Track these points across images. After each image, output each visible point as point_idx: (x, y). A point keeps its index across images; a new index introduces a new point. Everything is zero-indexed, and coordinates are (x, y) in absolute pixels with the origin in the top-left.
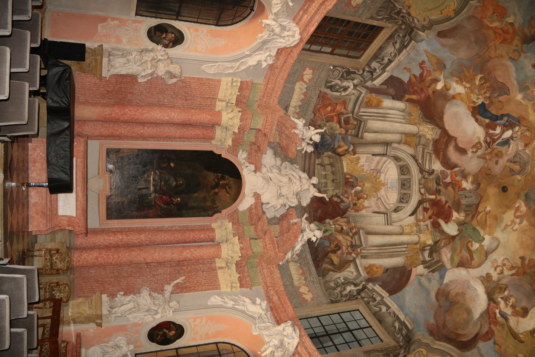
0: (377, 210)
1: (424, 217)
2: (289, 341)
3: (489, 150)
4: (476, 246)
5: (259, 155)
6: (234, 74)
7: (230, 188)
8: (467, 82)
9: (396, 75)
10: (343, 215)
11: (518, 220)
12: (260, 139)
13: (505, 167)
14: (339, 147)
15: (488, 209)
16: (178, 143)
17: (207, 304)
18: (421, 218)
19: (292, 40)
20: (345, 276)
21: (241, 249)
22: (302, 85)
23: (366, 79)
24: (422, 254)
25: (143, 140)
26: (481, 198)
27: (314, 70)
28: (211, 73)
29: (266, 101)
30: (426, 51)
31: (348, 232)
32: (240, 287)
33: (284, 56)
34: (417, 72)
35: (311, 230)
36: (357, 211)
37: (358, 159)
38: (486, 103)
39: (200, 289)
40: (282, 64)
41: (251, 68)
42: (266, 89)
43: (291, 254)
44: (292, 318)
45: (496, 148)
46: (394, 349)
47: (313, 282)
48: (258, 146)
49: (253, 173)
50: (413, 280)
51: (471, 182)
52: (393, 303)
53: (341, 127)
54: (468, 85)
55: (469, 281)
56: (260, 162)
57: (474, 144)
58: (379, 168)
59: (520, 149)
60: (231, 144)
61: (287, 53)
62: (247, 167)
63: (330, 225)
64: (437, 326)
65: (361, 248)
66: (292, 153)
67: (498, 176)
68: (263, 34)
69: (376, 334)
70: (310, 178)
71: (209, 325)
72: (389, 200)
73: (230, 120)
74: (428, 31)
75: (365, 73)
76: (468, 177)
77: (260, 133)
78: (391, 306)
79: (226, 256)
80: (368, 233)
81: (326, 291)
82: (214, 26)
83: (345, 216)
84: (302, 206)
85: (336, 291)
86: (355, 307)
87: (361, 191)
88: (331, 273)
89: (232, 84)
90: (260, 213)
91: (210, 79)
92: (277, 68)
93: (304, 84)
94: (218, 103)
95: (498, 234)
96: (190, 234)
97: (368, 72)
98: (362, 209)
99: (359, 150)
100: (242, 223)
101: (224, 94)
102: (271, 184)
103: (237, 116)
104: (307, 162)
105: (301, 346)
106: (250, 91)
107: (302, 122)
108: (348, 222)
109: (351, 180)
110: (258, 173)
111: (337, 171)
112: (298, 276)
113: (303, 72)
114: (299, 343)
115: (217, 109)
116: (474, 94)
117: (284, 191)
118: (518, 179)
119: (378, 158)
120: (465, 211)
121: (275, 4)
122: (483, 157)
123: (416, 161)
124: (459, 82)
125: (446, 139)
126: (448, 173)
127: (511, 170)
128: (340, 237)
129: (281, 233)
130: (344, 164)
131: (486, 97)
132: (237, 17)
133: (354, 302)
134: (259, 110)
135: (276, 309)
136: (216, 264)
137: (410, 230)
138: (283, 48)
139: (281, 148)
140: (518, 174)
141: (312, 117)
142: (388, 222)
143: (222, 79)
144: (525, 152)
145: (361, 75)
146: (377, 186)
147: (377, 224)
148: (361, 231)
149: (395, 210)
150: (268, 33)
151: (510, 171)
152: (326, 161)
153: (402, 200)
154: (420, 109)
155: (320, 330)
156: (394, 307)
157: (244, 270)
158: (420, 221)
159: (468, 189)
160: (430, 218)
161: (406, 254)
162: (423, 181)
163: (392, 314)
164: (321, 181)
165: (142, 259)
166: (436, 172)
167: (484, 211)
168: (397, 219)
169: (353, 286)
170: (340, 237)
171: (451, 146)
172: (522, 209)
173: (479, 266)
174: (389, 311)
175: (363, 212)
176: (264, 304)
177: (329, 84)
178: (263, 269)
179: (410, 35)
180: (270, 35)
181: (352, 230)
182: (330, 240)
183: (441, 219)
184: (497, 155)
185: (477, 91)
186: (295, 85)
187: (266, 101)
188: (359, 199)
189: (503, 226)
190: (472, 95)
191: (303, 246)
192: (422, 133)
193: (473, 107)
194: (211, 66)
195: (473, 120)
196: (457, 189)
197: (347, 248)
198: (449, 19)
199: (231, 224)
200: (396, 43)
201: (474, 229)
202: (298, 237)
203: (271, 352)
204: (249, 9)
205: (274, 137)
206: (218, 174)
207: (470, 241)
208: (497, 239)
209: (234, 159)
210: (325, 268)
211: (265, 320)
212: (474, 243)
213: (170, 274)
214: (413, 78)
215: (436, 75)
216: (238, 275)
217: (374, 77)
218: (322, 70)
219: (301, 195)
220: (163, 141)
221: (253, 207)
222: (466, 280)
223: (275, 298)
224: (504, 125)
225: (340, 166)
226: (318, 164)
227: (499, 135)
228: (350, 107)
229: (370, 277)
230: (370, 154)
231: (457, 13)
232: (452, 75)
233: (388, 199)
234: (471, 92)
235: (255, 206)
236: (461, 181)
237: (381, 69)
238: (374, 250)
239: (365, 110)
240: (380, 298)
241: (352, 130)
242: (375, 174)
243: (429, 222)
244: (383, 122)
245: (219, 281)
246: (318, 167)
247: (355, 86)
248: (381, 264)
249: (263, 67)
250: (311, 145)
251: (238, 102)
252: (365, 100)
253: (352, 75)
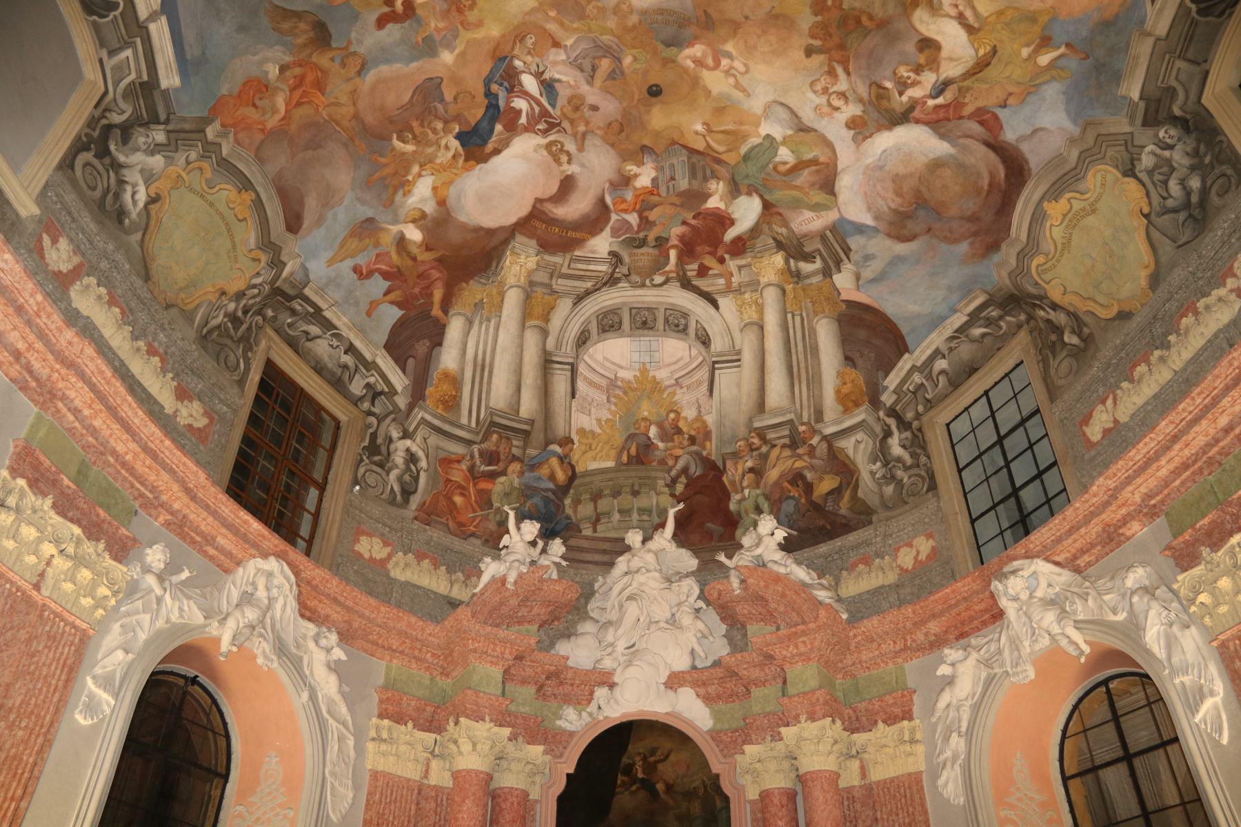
0: (705, 386)
1: (720, 275)
2: (1043, 584)
3: (566, 124)
4: (785, 154)
5: (569, 676)
6: (359, 736)
7: (653, 752)
8: (407, 170)
9: (383, 338)
10: (719, 468)
11: (725, 62)
12: (529, 671)
13: (605, 90)
14: (552, 477)
15: (699, 127)
17: (964, 806)
18: (722, 281)
19: (279, 580)
20: (866, 458)
21: (812, 718)
22: (397, 564)
23: (391, 408)
24: (808, 277)
26: (676, 144)
27: (359, 533)
28: (351, 795)
29: (433, 655)
30: (330, 262)
31: (760, 455)
32: (911, 719)
33: (320, 601)
34: (378, 285)
35: (758, 545)
36: (707, 435)
37: (582, 432)
38: (457, 130)
40: (339, 609)
41: (347, 689)
42: (402, 652)
43: (820, 590)
44: (984, 580)
45: (561, 109)
46: (1036, 334)
47: (886, 536)
48: (548, 678)
49: (617, 690)
50: (869, 296)
51: (639, 167)
52: (924, 344)
53: (503, 473)
54: (416, 169)
55: (867, 167)
56: (587, 672)
57: (550, 159)
58: (604, 382)
59: (563, 57)
60: (540, 748)
61: (314, 593)
62: (600, 708)
63: (744, 499)
64: (975, 234)
65: (797, 423)
66: (564, 591)
67: (625, 104)
68: (258, 652)
69: (1003, 378)
70: (628, 549)
71: (1019, 799)
72: (681, 359)
73: (479, 747)
74: (283, 252)
75: (376, 410)
76: (626, 174)
77: (513, 671)
78: (934, 347)
79: (832, 758)
80: (761, 406)
81: (906, 503)
82: (229, 786)
83: (720, 464)
84: (699, 570)
85: (905, 480)
86: (941, 432)
87: (660, 425)
88: (860, 494)
89: (385, 741)
90: (719, 672)
91: (368, 801)
92: (349, 622)
93: (394, 559)
94: (433, 780)
95: (756, 104)
97: (373, 404)
98: (704, 422)
99: (560, 429)
100: (744, 720)
101: (409, 764)
102: (644, 646)
103: (468, 729)
104: (588, 557)
105: (1054, 554)
106: (405, 694)
107: (488, 565)
108: (736, 455)
109: (633, 451)
110: (616, 679)
111: (611, 483)
112: (873, 574)
113: (364, 558)
114: (1047, 560)
115: (448, 783)
116: (436, 157)
117: (661, 612)
118: (632, 63)
119: (581, 385)
120: (705, 179)
121: (181, 616)
122: (581, 140)
123: (588, 293)
124: (407, 188)
125: (538, 224)
126: (618, 220)
127: (612, 76)
128: (773, 475)
129: (768, 617)
130: (594, 466)
131: (443, 130)
132: (209, 720)
133: (929, 435)
134: (454, 674)
135: (963, 623)
136: (854, 787)
137: (751, 307)
138: (299, 604)
139: (553, 621)
140: (621, 63)
141: (478, 542)
142: (734, 359)
143: (369, 767)
144: (571, 46)
145: (380, 420)
146: (647, 386)
147: (739, 386)
148: (757, 424)
149: (704, 343)
150: (256, 640)
151: (614, 79)
152: (586, 510)
153: (681, 327)
154: (467, 283)
155: (1006, 514)
156: (937, 339)
157: (866, 710)
158: (729, 284)
159: (653, 174)
160: (722, 261)
161: (808, 316)
162: (636, 278)
163: (953, 345)
164: (635, 523)
166: (616, 248)
167: (704, 136)
168: (726, 339)
169: (890, 441)
170: (773, 475)
171: (555, 211)
172: (699, 54)
173: (829, 145)
174: (946, 353)
175: (710, 420)
176: (951, 654)
177: (399, 498)
178: (861, 662)
179: (290, 298)
180: (261, 635)
181: (754, 447)
182: (780, 498)
183: (724, 234)
184: (577, 109)
185: (430, 150)
186: (395, 580)
187: (433, 655)
188: (679, 431)
189: (737, 94)
190: (438, 161)
191: (799, 563)
192: (522, 278)
193: (466, 160)
194: (332, 795)
195: (496, 161)
196: (655, 199)
197: (800, 457)
198: (258, 204)
199: (747, 748)
200: (307, 333)
201: (746, 158)
202: (777, 574)
203: (1078, 629)
204: (190, 688)
205: (527, 636)
206: (619, 782)
207: (775, 168)
208: (768, 107)
209: (580, 738)
210: (850, 509)
211: (992, 649)
212: (777, 159)
214: (392, 296)
215: (387, 241)
216: (881, 725)
217: (386, 390)
218: (361, 511)
219: (671, 572)
221: (702, 691)
222: (864, 173)
223: (934, 627)
224: (510, 90)
225: (599, 477)
226: (595, 531)
227: (532, 102)
228: (457, 449)
229: (866, 398)
230: (571, 403)
231: (246, 184)
232: (389, 204)
233: (678, 361)
234: (431, 161)
235: (699, 686)
236: (635, 188)
237: (368, 371)
238: (800, 392)
239: (465, 412)
240: (916, 373)
241: (512, 445)
242: (618, 392)
243: (732, 264)
244: (496, 371)
245: (897, 777)
246: (603, 530)
247: (406, 435)
248: (834, 373)
249: (344, 658)
250: (546, 544)
251: (433, 725)
252: (440, 411)
253: (379, 441)
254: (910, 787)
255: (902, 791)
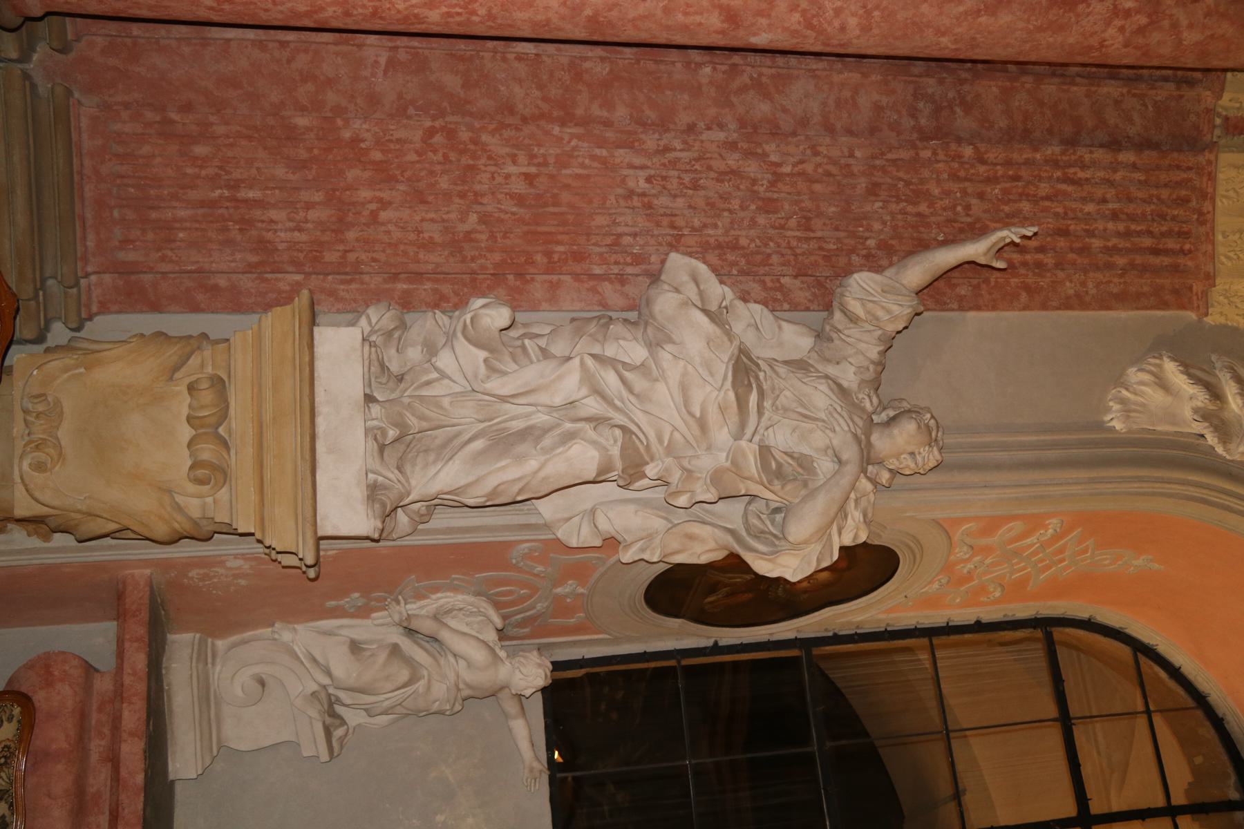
17: (1100, 426)
39: (1069, 288)
165: (714, 21)
213: (873, 131)
254: (1175, 269)
255: (1171, 244)
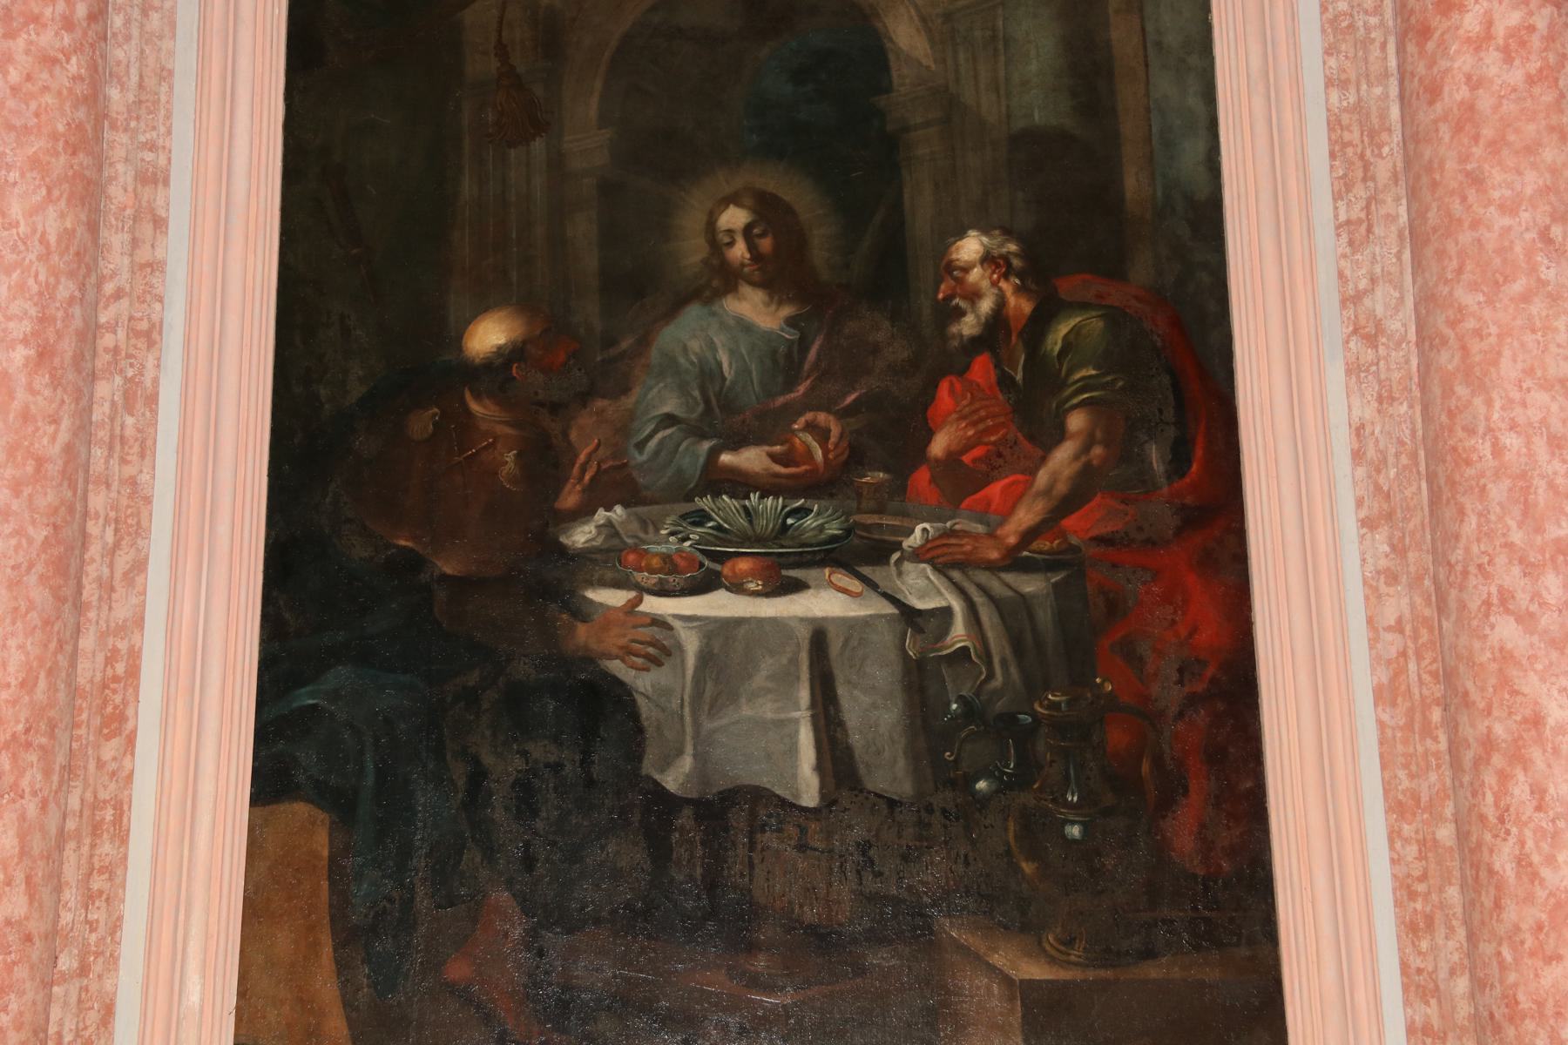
16: (175, 249)
25: (117, 723)
96: (1481, 42)
220: (146, 449)
